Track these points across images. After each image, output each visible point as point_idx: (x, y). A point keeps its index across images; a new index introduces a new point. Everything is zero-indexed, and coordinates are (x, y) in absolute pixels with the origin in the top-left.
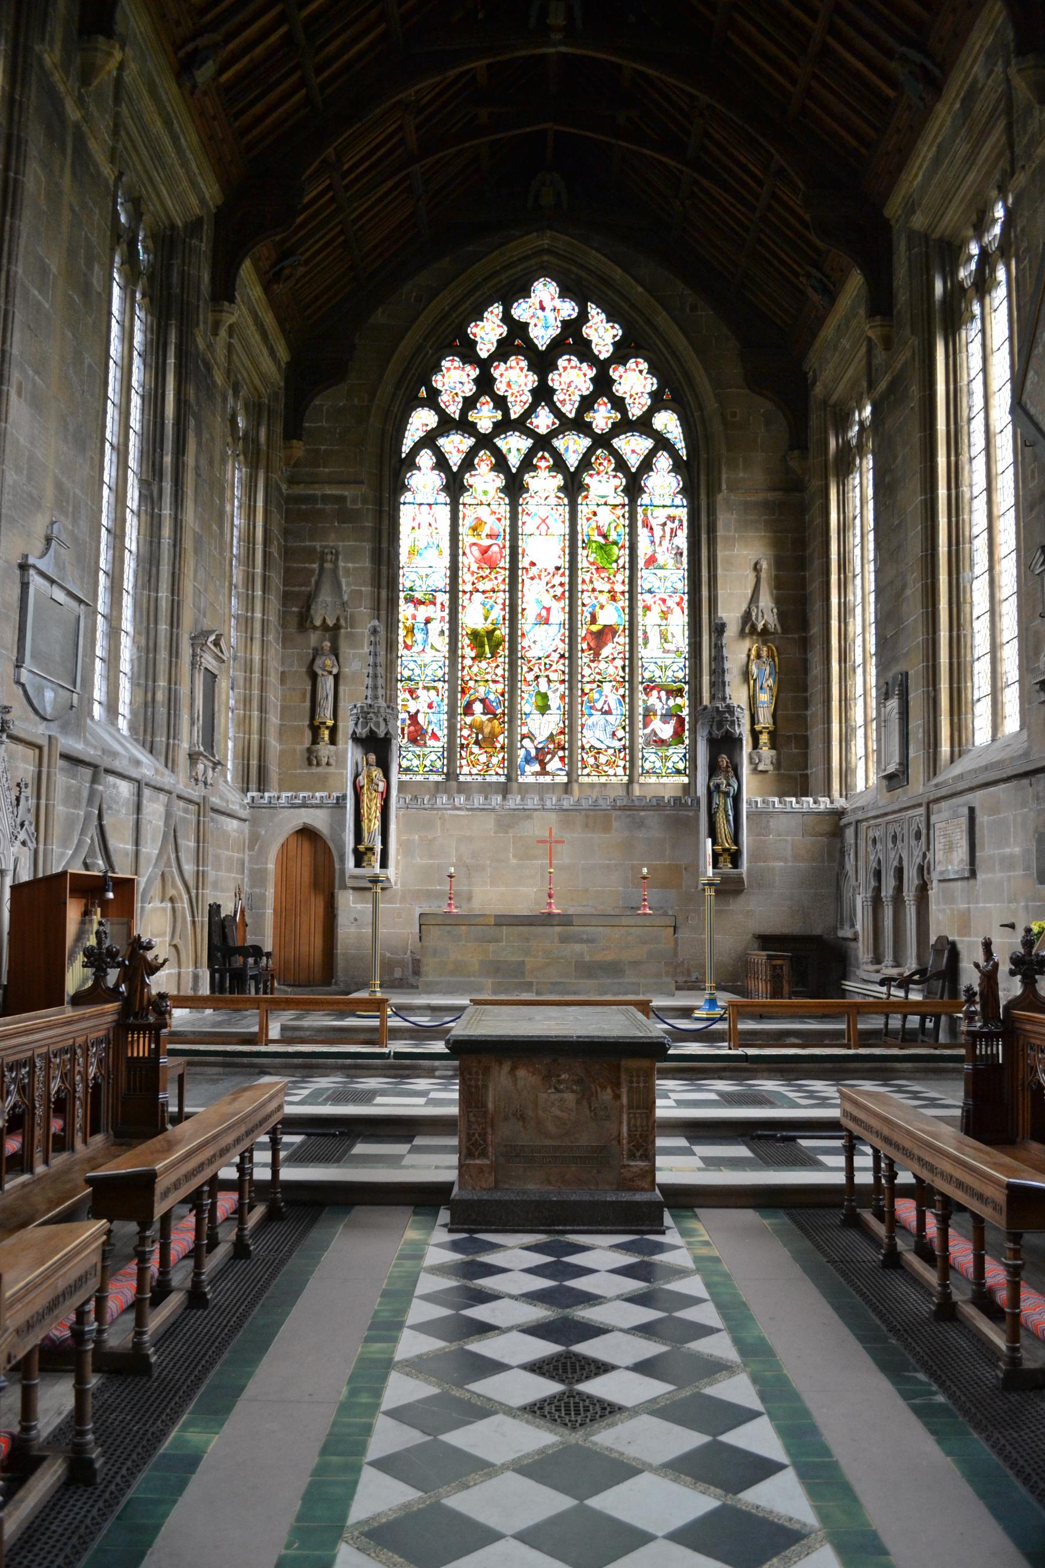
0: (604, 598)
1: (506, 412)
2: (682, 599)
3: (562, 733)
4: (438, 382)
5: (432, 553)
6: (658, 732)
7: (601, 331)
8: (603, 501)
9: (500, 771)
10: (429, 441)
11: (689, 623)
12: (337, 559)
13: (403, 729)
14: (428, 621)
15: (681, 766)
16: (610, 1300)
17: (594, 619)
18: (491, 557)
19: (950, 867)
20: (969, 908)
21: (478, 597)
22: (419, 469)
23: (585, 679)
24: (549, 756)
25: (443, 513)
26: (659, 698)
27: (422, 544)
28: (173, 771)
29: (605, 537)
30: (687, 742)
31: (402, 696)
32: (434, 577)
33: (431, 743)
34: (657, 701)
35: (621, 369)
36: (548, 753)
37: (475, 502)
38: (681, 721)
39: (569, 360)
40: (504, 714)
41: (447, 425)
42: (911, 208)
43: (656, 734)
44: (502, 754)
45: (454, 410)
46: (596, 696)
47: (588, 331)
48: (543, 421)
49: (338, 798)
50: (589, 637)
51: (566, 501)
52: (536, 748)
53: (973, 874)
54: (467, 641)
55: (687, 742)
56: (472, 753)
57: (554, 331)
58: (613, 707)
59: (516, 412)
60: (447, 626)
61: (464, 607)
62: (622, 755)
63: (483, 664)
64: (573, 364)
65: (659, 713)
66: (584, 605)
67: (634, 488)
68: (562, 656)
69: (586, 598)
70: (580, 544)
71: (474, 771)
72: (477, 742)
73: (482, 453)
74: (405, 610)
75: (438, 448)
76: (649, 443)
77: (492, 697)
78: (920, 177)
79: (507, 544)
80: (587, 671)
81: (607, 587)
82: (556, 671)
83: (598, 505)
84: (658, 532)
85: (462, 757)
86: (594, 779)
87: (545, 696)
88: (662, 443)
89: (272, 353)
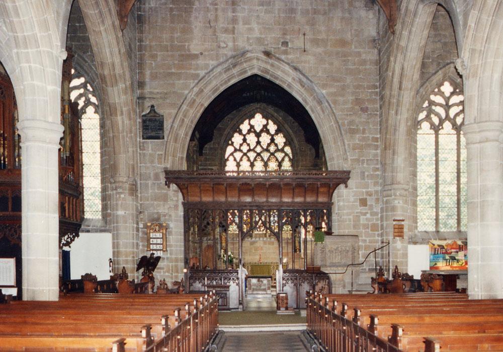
10: (232, 154)
41: (236, 150)
45: (238, 147)
53: (357, 236)
57: (261, 127)
76: (283, 154)
88: (286, 155)
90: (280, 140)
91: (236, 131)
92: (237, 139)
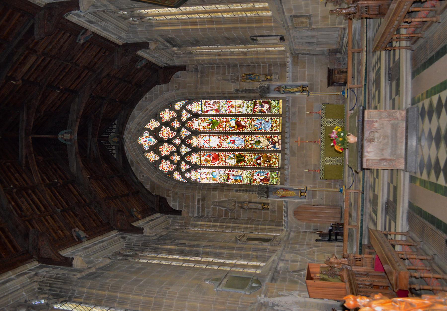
0: (228, 124)
1: (174, 152)
2: (228, 102)
3: (267, 137)
4: (166, 171)
5: (215, 174)
6: (267, 108)
7: (152, 125)
8: (200, 124)
9: (278, 155)
10: (182, 174)
11: (235, 99)
12: (216, 201)
13: (265, 183)
14: (233, 175)
15: (277, 102)
16: (439, 124)
17: (234, 127)
18: (215, 157)
19: (308, 22)
20: (321, 16)
21: (227, 161)
22: (190, 177)
23: (251, 130)
24: (273, 141)
25: (203, 170)
26: (257, 108)
27: (211, 176)
28: (276, 250)
29: (210, 124)
30: (270, 100)
31: (255, 183)
32: (221, 173)
33: (269, 175)
34: (258, 109)
35: (163, 119)
36: (272, 141)
37: (200, 161)
38: (263, 102)
39: (160, 134)
40: (261, 154)
41: (178, 169)
42: (120, 37)
43: (267, 109)
44: (273, 155)
45: (174, 167)
46: (256, 127)
47: (152, 128)
49: (285, 203)
50: (239, 128)
51: (200, 135)
52: (271, 144)
54: (240, 164)
55: (270, 100)
56: (272, 163)
58: (259, 122)
59: (174, 149)
60: (235, 170)
61: (230, 165)
62: (273, 119)
63: (246, 159)
64: (161, 133)
65: (261, 108)
66: (230, 130)
67: (196, 115)
68: (244, 136)
69: (228, 129)
70: (212, 131)
71: (277, 163)
72: (269, 162)
73: (186, 159)
74: (230, 182)
75: (184, 171)
77: (256, 157)
78: (112, 35)
79: (212, 152)
80: (249, 129)
81: (225, 124)
82: (249, 138)
83: (201, 126)
84: (209, 109)
85: (274, 166)
86: (280, 127)
87: (256, 142)
88: (183, 107)
89: (157, 218)
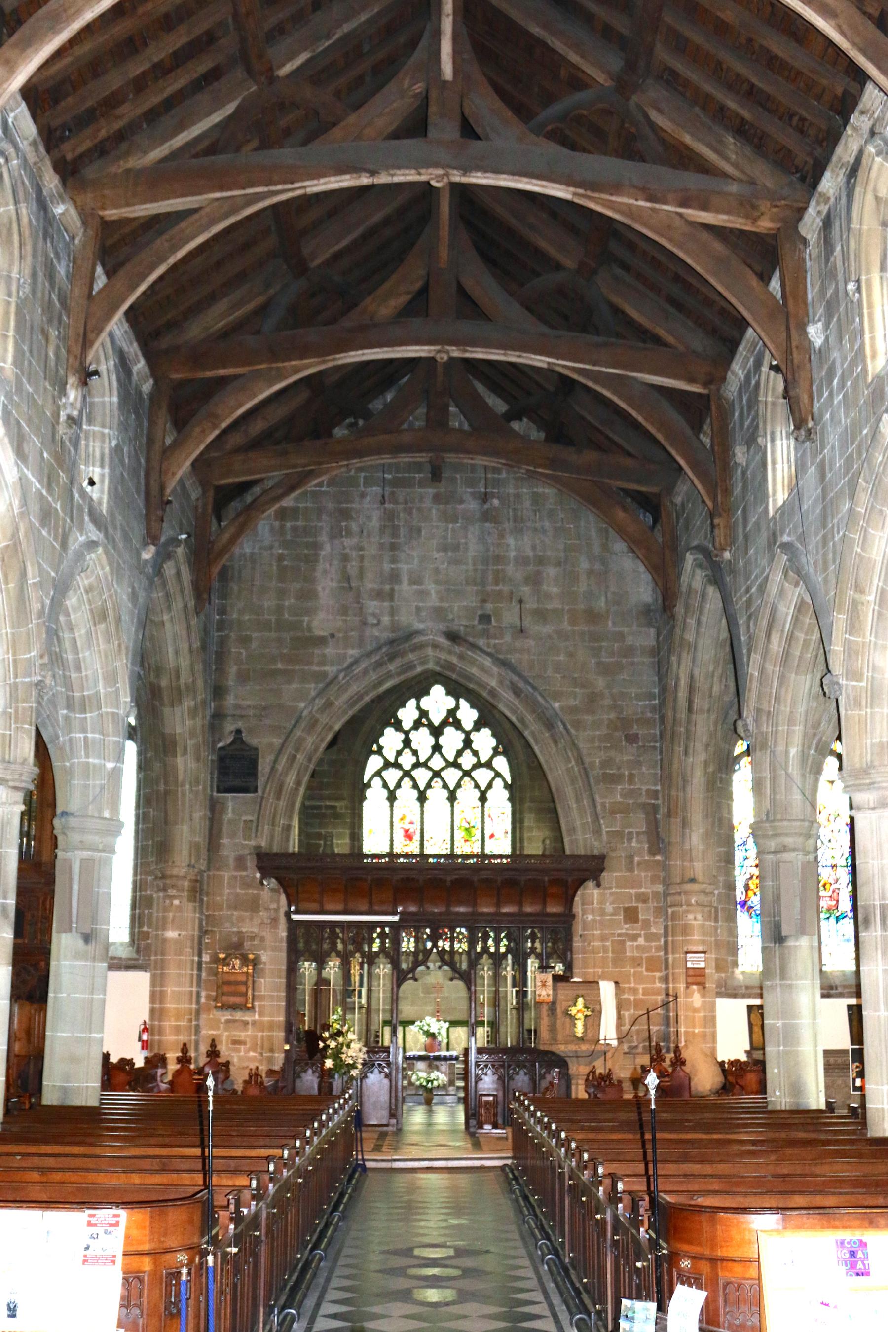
10: (378, 773)
41: (387, 765)
48: (437, 763)
88: (498, 774)
90: (485, 741)
91: (389, 724)
92: (390, 740)
